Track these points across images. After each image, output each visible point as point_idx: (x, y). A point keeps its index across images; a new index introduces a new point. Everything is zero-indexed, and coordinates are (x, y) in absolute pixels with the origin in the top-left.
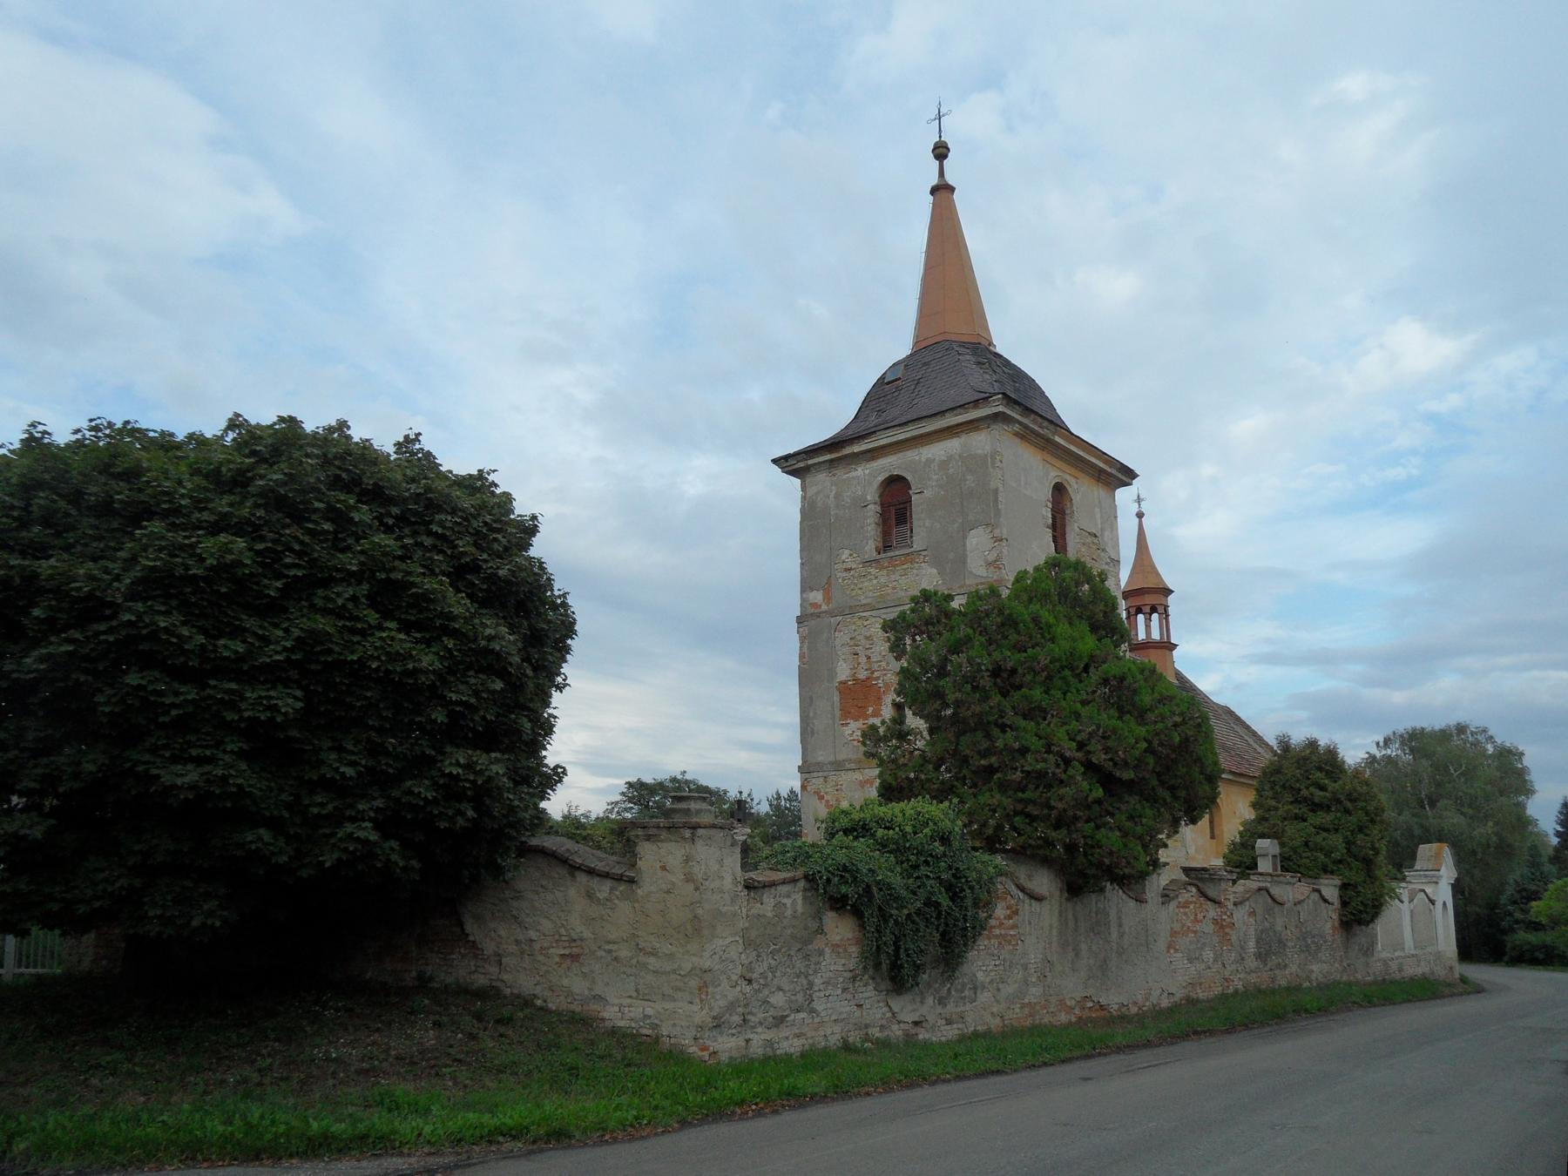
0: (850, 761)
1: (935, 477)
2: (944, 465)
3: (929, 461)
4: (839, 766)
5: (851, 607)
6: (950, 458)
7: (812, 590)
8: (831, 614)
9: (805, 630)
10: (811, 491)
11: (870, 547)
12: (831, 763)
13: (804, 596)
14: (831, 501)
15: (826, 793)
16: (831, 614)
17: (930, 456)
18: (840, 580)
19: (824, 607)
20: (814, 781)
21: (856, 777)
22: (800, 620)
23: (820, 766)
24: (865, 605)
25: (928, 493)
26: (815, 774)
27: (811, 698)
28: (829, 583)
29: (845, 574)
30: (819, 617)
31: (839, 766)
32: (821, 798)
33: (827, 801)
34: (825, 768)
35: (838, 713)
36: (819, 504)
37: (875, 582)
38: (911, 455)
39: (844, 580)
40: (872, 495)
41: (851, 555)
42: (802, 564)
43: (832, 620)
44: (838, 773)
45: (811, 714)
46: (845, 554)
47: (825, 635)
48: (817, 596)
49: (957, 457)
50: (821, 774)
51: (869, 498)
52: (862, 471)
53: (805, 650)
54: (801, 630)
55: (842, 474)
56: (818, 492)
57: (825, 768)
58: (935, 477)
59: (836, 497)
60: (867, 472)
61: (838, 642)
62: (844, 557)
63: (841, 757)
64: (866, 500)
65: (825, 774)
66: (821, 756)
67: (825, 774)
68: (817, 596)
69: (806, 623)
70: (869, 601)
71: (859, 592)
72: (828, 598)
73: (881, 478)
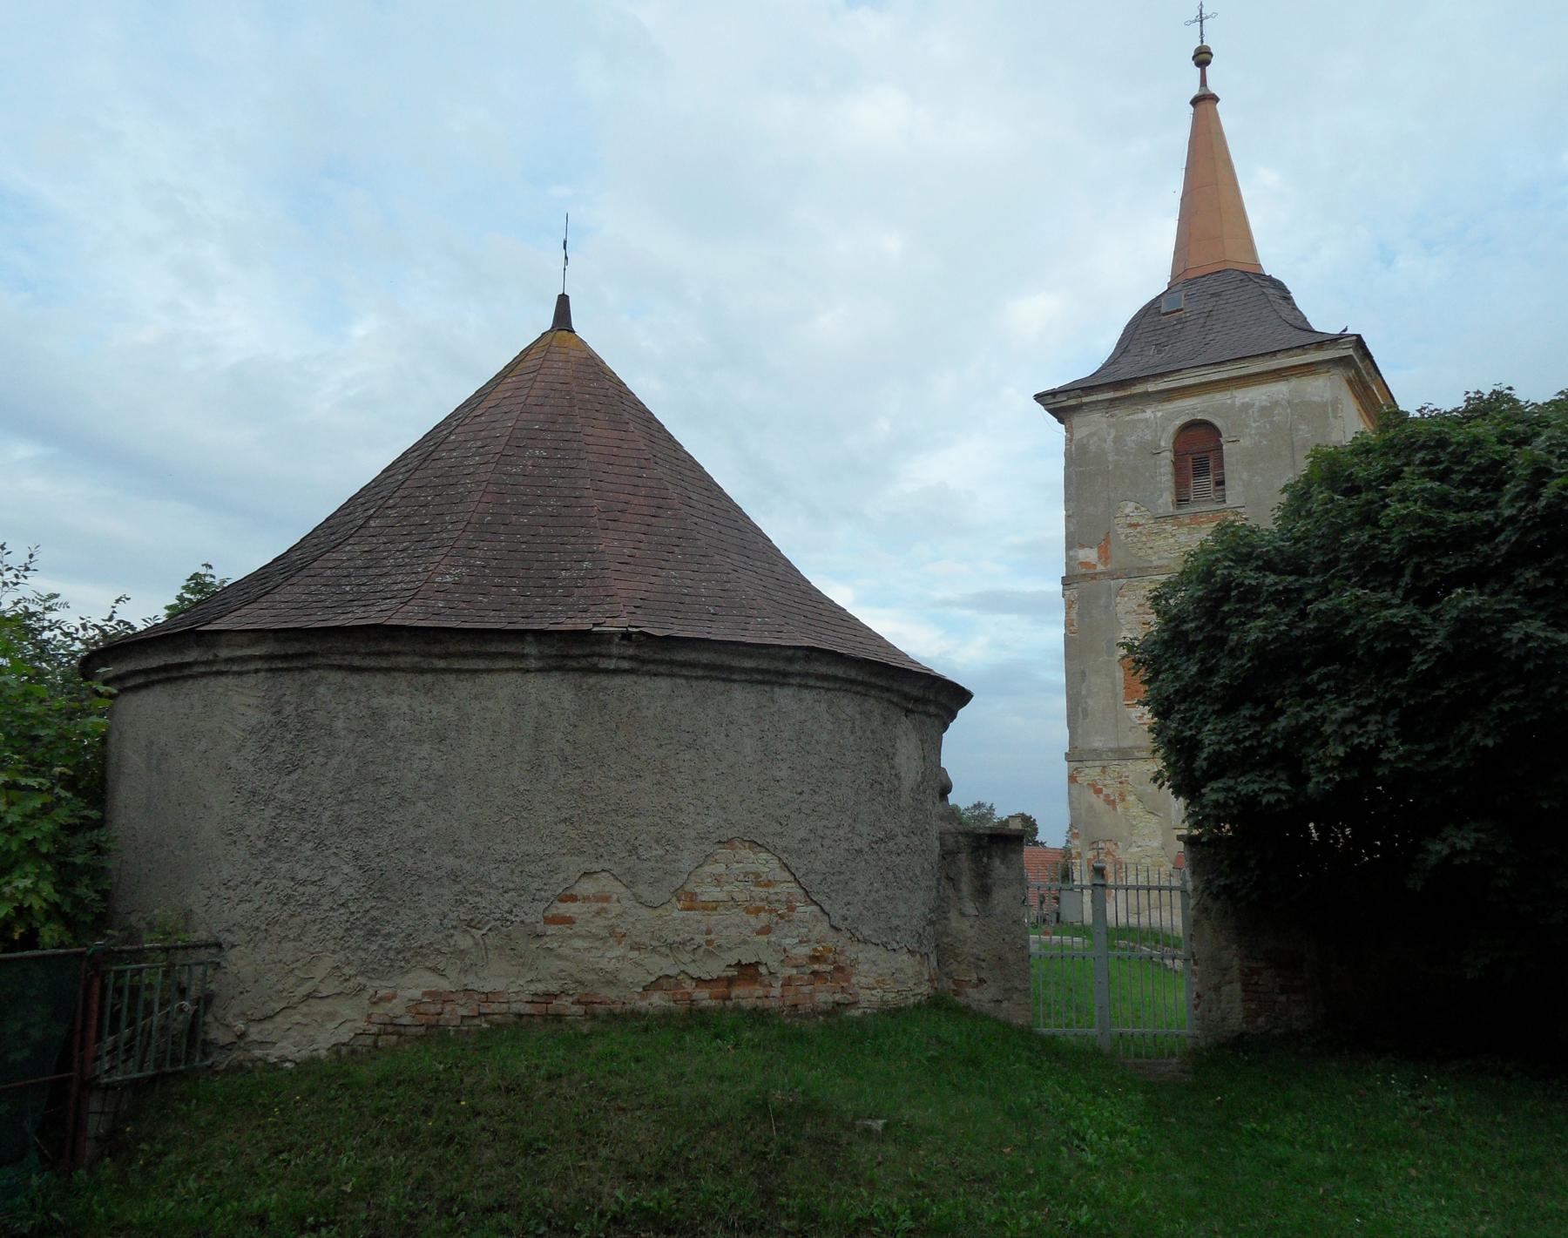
0: (1139, 748)
1: (1254, 425)
2: (1265, 411)
3: (1246, 407)
4: (1124, 754)
5: (1139, 569)
6: (1276, 404)
7: (1082, 546)
8: (1111, 575)
9: (1074, 593)
10: (1081, 433)
11: (1166, 499)
12: (1111, 750)
13: (1071, 553)
14: (1109, 445)
15: (1105, 786)
16: (1111, 575)
17: (1247, 400)
18: (1122, 537)
19: (1100, 568)
20: (1087, 771)
21: (1148, 767)
22: (1067, 582)
23: (1097, 754)
24: (1161, 567)
25: (1245, 442)
26: (1090, 763)
27: (1083, 673)
28: (1107, 540)
29: (1129, 530)
30: (1093, 578)
31: (1124, 754)
32: (1098, 792)
33: (1107, 796)
34: (1104, 756)
35: (1121, 691)
36: (1093, 448)
37: (1172, 540)
38: (1220, 398)
39: (1127, 536)
40: (1166, 441)
41: (1137, 509)
42: (1068, 517)
43: (1112, 582)
44: (1124, 762)
45: (1084, 692)
46: (1129, 508)
47: (1102, 601)
48: (1089, 555)
49: (1284, 403)
50: (1098, 763)
51: (1163, 444)
52: (1150, 413)
53: (1074, 616)
54: (1067, 593)
55: (1123, 415)
56: (1090, 435)
57: (1104, 756)
58: (1254, 425)
59: (1116, 440)
60: (1159, 414)
61: (1120, 609)
62: (1127, 511)
63: (1127, 743)
64: (1159, 447)
65: (1105, 763)
66: (1097, 743)
67: (1105, 763)
68: (1089, 555)
69: (1075, 585)
70: (1165, 562)
71: (1150, 551)
72: (1105, 556)
73: (1179, 422)
